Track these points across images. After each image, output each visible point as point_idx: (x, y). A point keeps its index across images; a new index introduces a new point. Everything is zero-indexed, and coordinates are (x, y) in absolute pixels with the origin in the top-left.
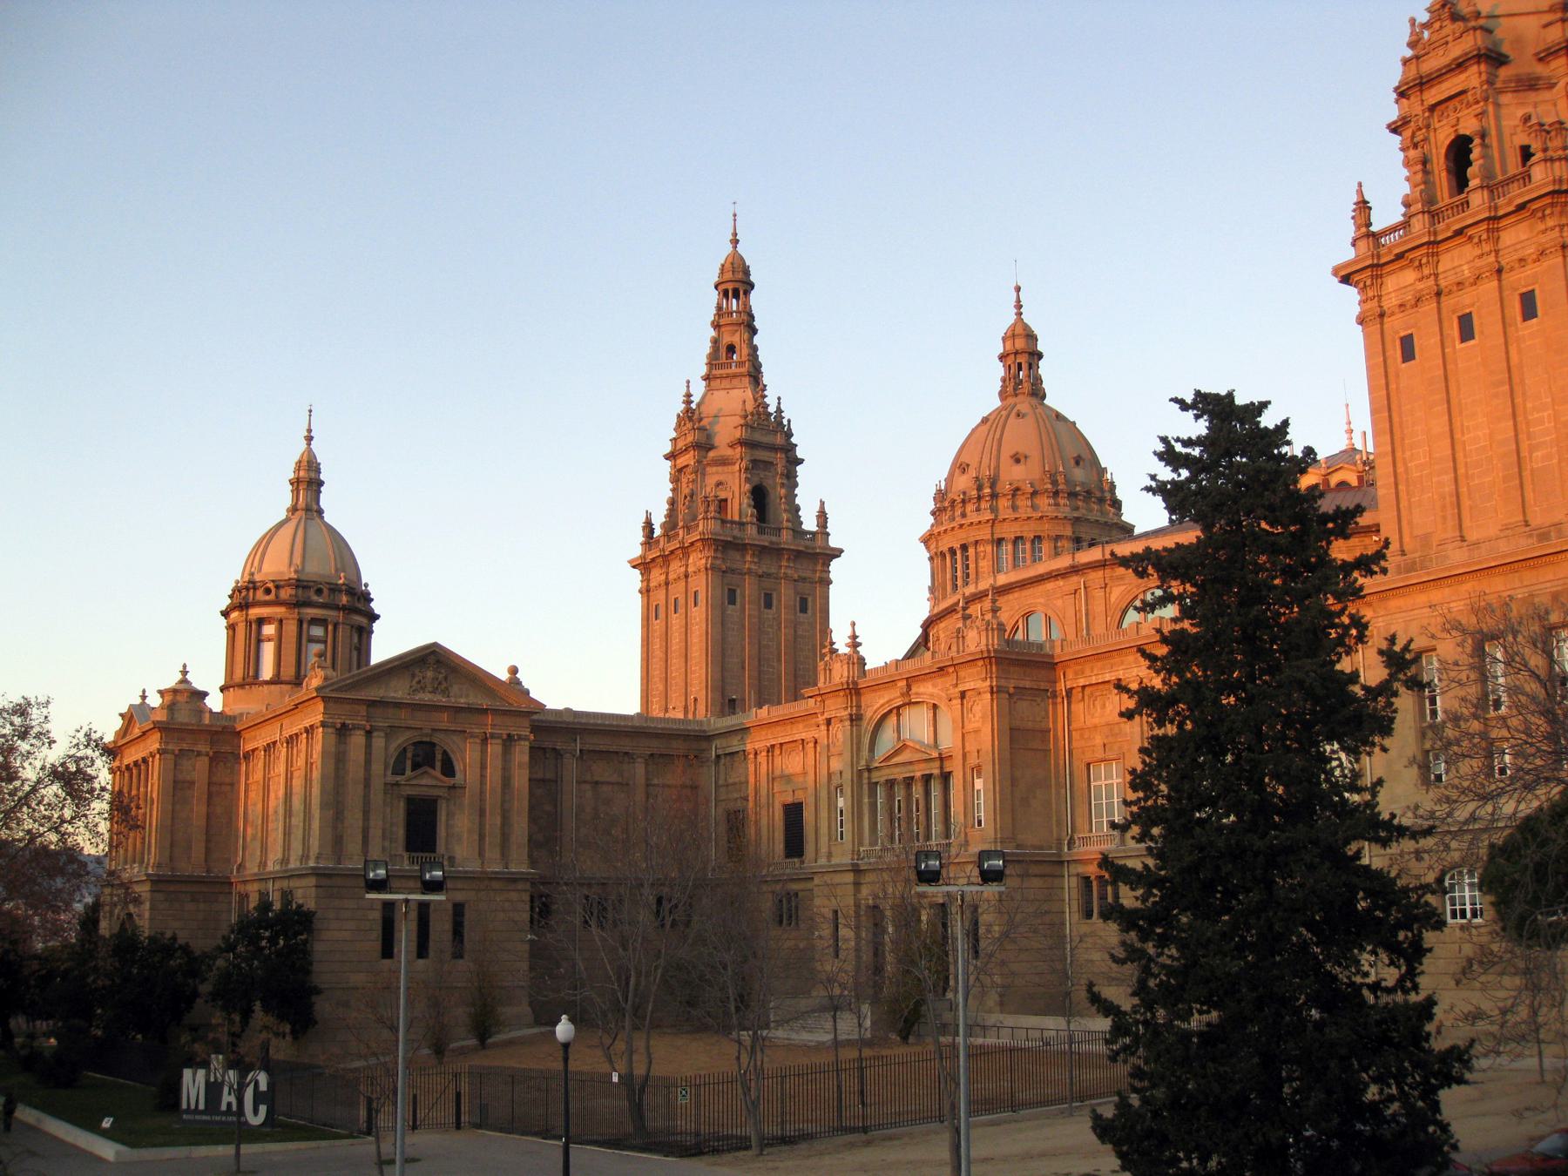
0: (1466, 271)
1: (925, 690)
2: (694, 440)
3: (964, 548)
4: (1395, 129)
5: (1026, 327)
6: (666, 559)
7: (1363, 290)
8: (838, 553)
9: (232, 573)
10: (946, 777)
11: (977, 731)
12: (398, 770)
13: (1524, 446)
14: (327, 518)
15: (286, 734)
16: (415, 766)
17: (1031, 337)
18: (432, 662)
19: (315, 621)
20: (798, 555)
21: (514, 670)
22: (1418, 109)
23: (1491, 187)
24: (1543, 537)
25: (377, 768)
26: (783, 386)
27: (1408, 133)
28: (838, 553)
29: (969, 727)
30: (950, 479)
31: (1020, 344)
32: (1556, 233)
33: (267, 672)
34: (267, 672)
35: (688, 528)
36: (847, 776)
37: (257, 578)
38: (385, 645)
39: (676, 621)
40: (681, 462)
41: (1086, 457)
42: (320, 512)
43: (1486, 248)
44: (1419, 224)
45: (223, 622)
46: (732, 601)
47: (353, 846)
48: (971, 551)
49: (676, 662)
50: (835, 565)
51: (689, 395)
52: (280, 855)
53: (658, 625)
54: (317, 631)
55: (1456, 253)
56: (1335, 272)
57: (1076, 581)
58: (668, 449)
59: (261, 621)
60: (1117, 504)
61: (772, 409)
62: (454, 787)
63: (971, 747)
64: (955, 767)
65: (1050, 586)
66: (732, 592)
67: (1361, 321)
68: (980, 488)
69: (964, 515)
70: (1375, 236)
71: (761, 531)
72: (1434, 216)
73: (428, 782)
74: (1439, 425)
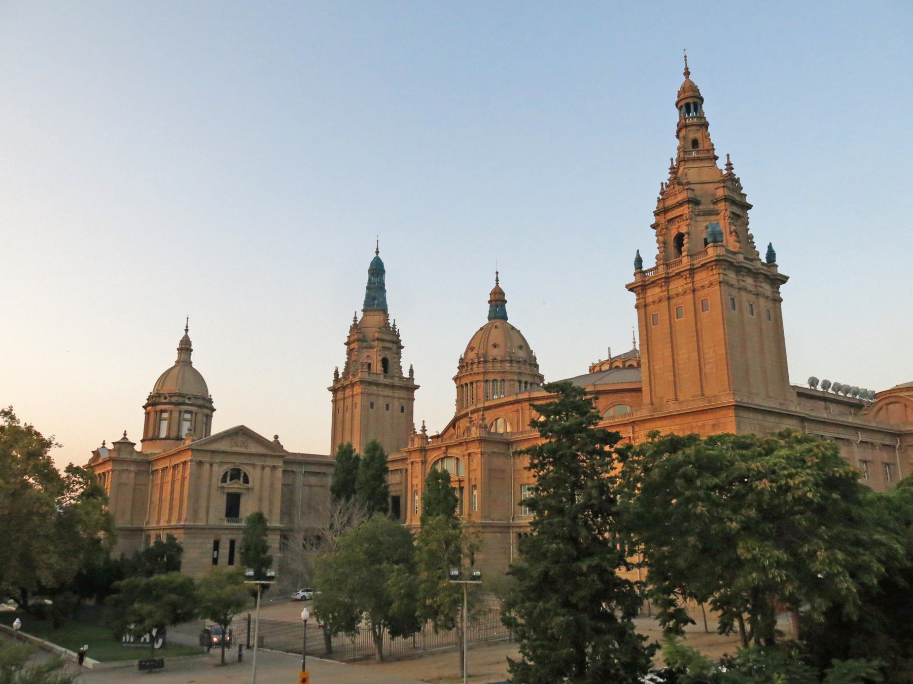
0: (680, 290)
1: (454, 452)
2: (358, 338)
3: (472, 383)
4: (653, 227)
5: (500, 289)
6: (344, 388)
7: (638, 295)
8: (417, 387)
9: (149, 388)
10: (461, 489)
11: (475, 470)
12: (224, 480)
13: (702, 363)
14: (194, 366)
15: (173, 464)
16: (231, 480)
17: (503, 294)
18: (242, 433)
19: (187, 412)
21: (276, 437)
22: (663, 221)
23: (690, 255)
24: (709, 401)
25: (214, 480)
26: (397, 314)
27: (659, 229)
28: (417, 387)
29: (472, 468)
30: (466, 353)
31: (497, 297)
32: (717, 276)
33: (163, 434)
34: (163, 434)
35: (354, 375)
36: (419, 486)
37: (161, 392)
38: (218, 425)
41: (524, 345)
42: (191, 363)
43: (689, 280)
44: (661, 269)
45: (144, 411)
47: (202, 515)
48: (474, 385)
50: (416, 392)
51: (355, 318)
52: (167, 518)
54: (188, 416)
55: (676, 282)
56: (627, 286)
57: (517, 406)
58: (346, 340)
59: (162, 411)
60: (537, 366)
61: (391, 325)
62: (248, 489)
63: (472, 477)
64: (465, 485)
65: (506, 407)
67: (637, 307)
68: (479, 358)
69: (472, 369)
70: (645, 272)
71: (385, 377)
72: (667, 265)
73: (235, 486)
74: (668, 352)
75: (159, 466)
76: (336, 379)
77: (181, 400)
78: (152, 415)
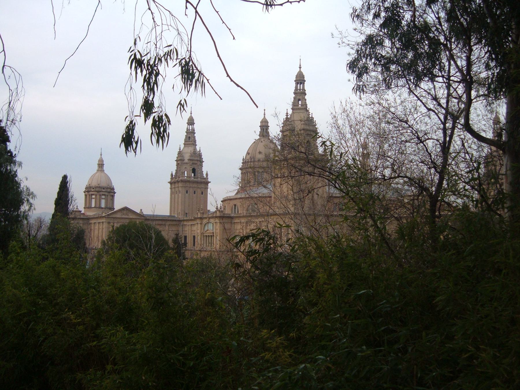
14: (105, 172)
18: (126, 209)
19: (103, 195)
20: (201, 183)
21: (141, 210)
26: (200, 145)
31: (264, 124)
33: (93, 205)
34: (93, 205)
39: (176, 195)
40: (178, 162)
42: (104, 171)
46: (187, 193)
49: (176, 204)
50: (209, 184)
53: (173, 196)
54: (103, 197)
59: (92, 195)
66: (187, 191)
68: (251, 159)
75: (92, 221)
76: (172, 178)
77: (100, 189)
78: (88, 196)
